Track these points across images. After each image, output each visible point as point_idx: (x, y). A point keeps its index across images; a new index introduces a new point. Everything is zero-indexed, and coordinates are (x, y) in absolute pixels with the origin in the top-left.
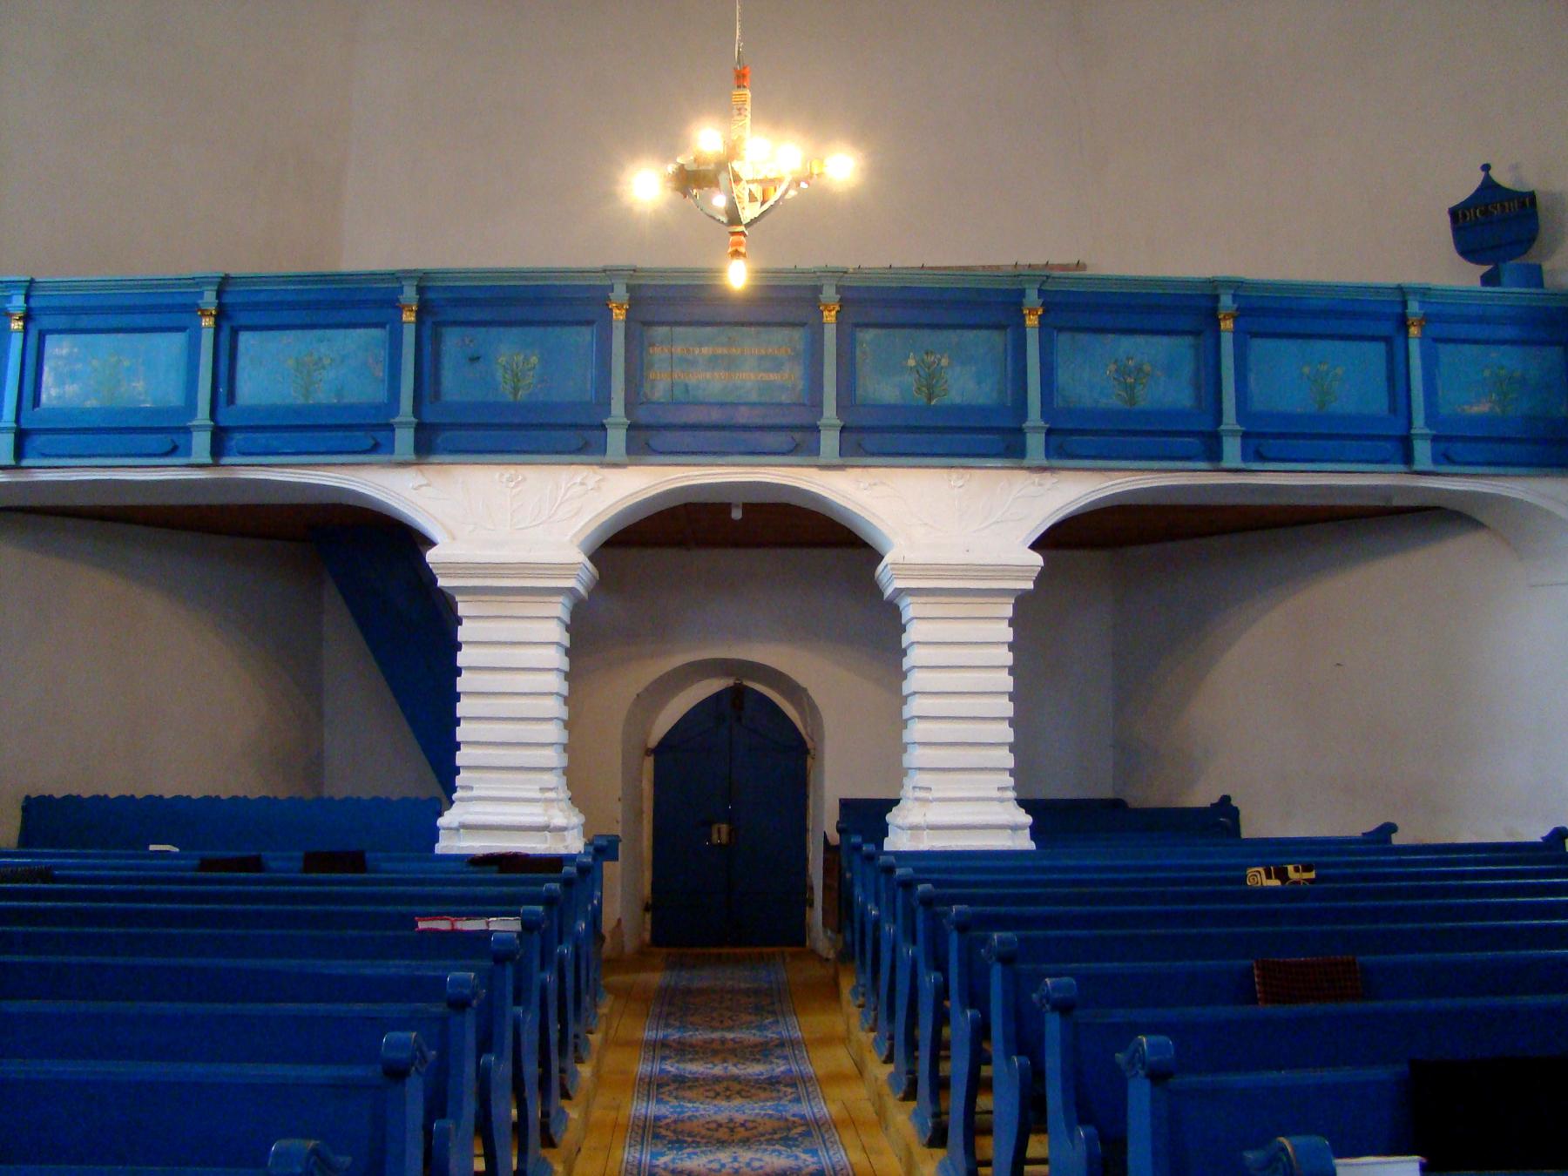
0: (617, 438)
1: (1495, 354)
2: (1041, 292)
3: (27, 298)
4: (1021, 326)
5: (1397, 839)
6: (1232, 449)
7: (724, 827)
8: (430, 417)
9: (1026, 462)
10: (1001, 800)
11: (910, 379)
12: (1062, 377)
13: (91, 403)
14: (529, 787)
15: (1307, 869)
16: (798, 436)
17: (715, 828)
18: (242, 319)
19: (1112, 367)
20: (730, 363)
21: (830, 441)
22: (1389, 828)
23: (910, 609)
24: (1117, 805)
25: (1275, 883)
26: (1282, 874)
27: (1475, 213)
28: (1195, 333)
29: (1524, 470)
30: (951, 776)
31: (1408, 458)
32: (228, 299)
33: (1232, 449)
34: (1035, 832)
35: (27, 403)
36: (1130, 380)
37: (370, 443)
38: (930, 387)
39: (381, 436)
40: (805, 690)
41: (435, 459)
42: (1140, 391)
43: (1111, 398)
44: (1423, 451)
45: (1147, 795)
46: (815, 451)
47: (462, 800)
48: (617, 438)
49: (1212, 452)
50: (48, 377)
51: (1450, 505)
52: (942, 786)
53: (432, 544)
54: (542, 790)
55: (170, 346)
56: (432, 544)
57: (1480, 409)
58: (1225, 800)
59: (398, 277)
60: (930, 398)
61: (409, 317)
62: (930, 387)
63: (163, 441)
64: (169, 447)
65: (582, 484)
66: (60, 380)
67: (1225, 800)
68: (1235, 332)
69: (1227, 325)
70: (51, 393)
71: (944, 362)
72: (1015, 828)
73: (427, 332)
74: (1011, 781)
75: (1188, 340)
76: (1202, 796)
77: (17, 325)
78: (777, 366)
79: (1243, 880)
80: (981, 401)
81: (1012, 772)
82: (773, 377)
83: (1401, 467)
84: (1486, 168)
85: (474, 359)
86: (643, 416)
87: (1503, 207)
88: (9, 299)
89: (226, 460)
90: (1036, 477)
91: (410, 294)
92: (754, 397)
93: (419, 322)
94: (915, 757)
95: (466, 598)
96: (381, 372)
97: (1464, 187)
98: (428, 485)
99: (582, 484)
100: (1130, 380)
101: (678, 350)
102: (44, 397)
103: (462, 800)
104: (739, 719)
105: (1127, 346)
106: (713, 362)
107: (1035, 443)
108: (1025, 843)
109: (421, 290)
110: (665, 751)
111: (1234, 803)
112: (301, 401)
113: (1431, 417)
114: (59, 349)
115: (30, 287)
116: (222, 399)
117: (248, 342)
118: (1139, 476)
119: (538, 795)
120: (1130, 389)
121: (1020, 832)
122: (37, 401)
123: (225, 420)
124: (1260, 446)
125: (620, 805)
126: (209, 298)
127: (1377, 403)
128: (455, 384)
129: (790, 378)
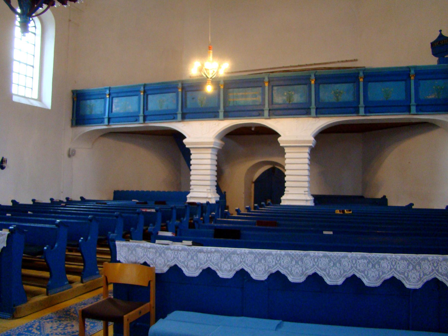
0: (221, 114)
1: (436, 82)
2: (315, 75)
3: (109, 91)
4: (310, 84)
5: (413, 207)
6: (362, 110)
8: (185, 111)
9: (311, 116)
10: (305, 194)
11: (285, 98)
12: (321, 95)
13: (122, 111)
14: (205, 189)
15: (350, 211)
16: (260, 112)
18: (148, 93)
19: (333, 92)
20: (246, 96)
21: (266, 113)
22: (412, 205)
23: (286, 150)
24: (362, 197)
25: (341, 213)
26: (343, 212)
27: (437, 44)
28: (354, 82)
29: (444, 112)
31: (409, 111)
32: (146, 88)
33: (362, 110)
34: (315, 201)
35: (110, 112)
36: (337, 95)
37: (173, 117)
38: (290, 99)
39: (175, 116)
41: (186, 120)
42: (340, 97)
43: (333, 100)
44: (413, 109)
45: (369, 195)
46: (263, 115)
47: (192, 192)
48: (221, 114)
49: (356, 111)
50: (114, 107)
51: (429, 122)
53: (185, 137)
54: (207, 190)
55: (135, 98)
56: (185, 137)
57: (432, 97)
58: (384, 197)
59: (177, 82)
60: (290, 102)
61: (180, 90)
62: (290, 99)
63: (134, 119)
64: (135, 120)
65: (215, 124)
66: (116, 107)
67: (384, 197)
68: (364, 82)
69: (361, 80)
70: (115, 109)
71: (293, 93)
73: (184, 93)
75: (352, 84)
76: (380, 196)
77: (108, 96)
78: (255, 96)
79: (335, 212)
80: (301, 102)
82: (255, 99)
83: (408, 113)
84: (440, 31)
85: (193, 99)
86: (227, 109)
87: (444, 42)
88: (106, 91)
89: (146, 122)
90: (314, 119)
91: (180, 85)
92: (251, 104)
93: (182, 91)
95: (192, 149)
96: (175, 102)
97: (434, 37)
98: (185, 126)
99: (215, 124)
100: (337, 95)
101: (235, 94)
102: (113, 111)
103: (192, 192)
105: (337, 86)
106: (242, 96)
107: (313, 111)
108: (311, 203)
109: (182, 84)
110: (257, 183)
111: (387, 197)
112: (160, 109)
113: (417, 100)
114: (115, 100)
115: (110, 89)
116: (145, 110)
117: (150, 97)
118: (342, 118)
119: (206, 191)
120: (337, 97)
121: (308, 202)
122: (112, 112)
123: (146, 113)
124: (368, 111)
125: (244, 195)
126: (142, 89)
127: (402, 97)
128: (190, 104)
129: (259, 99)
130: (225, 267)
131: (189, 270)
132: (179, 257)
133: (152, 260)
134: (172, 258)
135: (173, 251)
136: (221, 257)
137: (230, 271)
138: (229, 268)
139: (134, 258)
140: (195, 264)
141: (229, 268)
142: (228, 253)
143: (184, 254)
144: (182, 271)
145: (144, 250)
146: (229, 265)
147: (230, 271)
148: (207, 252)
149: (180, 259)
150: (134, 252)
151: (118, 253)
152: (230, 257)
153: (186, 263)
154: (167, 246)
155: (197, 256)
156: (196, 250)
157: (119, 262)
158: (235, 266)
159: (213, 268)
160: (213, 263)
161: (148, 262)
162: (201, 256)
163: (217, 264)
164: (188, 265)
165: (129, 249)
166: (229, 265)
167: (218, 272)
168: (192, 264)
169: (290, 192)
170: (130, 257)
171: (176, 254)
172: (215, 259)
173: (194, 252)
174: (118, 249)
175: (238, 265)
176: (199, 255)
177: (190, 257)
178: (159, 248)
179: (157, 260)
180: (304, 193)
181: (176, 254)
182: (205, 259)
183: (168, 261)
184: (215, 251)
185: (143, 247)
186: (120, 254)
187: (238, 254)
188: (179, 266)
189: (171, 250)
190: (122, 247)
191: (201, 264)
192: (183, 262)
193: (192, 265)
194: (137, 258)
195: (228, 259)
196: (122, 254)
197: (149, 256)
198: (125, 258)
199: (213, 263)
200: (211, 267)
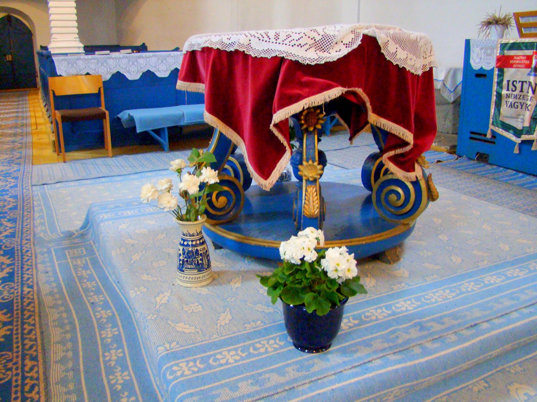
7: (10, 56)
10: (75, 41)
17: (7, 56)
30: (63, 35)
40: (28, 16)
52: (60, 38)
72: (79, 48)
74: (77, 36)
81: (78, 34)
94: (53, 30)
104: (10, 25)
130: (163, 68)
131: (131, 75)
132: (121, 64)
133: (95, 70)
134: (114, 66)
135: (114, 60)
136: (158, 60)
137: (167, 71)
138: (166, 69)
139: (75, 71)
140: (136, 68)
141: (166, 69)
142: (163, 56)
143: (125, 61)
144: (125, 76)
145: (85, 62)
146: (165, 66)
147: (167, 71)
148: (146, 57)
149: (121, 66)
150: (75, 65)
151: (57, 68)
152: (165, 59)
153: (128, 69)
154: (108, 56)
155: (137, 62)
156: (136, 56)
157: (61, 76)
158: (170, 66)
159: (152, 70)
160: (152, 66)
161: (90, 73)
162: (141, 61)
163: (155, 67)
164: (129, 70)
165: (69, 63)
166: (165, 66)
167: (156, 73)
168: (133, 69)
169: (58, 40)
170: (70, 71)
171: (118, 62)
172: (153, 62)
173: (134, 58)
174: (56, 64)
175: (173, 65)
176: (139, 60)
177: (131, 63)
178: (100, 58)
179: (100, 70)
180: (74, 39)
181: (118, 62)
182: (145, 64)
183: (110, 69)
184: (153, 56)
185: (84, 59)
186: (60, 68)
187: (172, 57)
188: (122, 72)
189: (113, 59)
190: (61, 61)
191: (141, 68)
192: (125, 69)
193: (133, 70)
194: (78, 71)
195: (164, 62)
196: (62, 68)
197: (90, 67)
198: (66, 71)
199: (152, 66)
200: (150, 69)
